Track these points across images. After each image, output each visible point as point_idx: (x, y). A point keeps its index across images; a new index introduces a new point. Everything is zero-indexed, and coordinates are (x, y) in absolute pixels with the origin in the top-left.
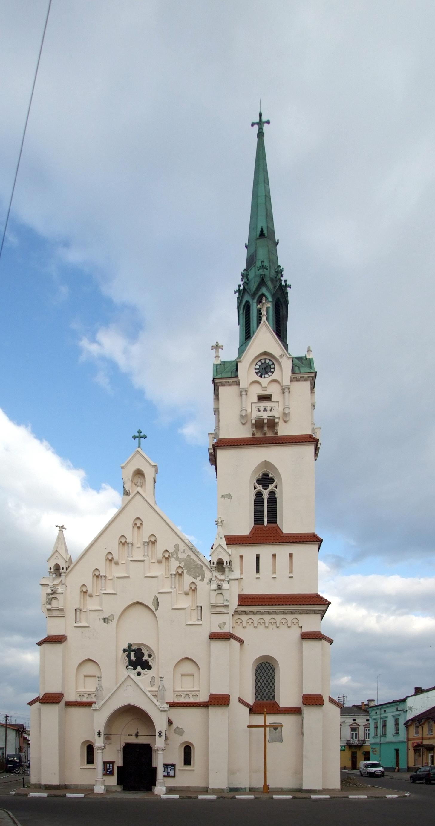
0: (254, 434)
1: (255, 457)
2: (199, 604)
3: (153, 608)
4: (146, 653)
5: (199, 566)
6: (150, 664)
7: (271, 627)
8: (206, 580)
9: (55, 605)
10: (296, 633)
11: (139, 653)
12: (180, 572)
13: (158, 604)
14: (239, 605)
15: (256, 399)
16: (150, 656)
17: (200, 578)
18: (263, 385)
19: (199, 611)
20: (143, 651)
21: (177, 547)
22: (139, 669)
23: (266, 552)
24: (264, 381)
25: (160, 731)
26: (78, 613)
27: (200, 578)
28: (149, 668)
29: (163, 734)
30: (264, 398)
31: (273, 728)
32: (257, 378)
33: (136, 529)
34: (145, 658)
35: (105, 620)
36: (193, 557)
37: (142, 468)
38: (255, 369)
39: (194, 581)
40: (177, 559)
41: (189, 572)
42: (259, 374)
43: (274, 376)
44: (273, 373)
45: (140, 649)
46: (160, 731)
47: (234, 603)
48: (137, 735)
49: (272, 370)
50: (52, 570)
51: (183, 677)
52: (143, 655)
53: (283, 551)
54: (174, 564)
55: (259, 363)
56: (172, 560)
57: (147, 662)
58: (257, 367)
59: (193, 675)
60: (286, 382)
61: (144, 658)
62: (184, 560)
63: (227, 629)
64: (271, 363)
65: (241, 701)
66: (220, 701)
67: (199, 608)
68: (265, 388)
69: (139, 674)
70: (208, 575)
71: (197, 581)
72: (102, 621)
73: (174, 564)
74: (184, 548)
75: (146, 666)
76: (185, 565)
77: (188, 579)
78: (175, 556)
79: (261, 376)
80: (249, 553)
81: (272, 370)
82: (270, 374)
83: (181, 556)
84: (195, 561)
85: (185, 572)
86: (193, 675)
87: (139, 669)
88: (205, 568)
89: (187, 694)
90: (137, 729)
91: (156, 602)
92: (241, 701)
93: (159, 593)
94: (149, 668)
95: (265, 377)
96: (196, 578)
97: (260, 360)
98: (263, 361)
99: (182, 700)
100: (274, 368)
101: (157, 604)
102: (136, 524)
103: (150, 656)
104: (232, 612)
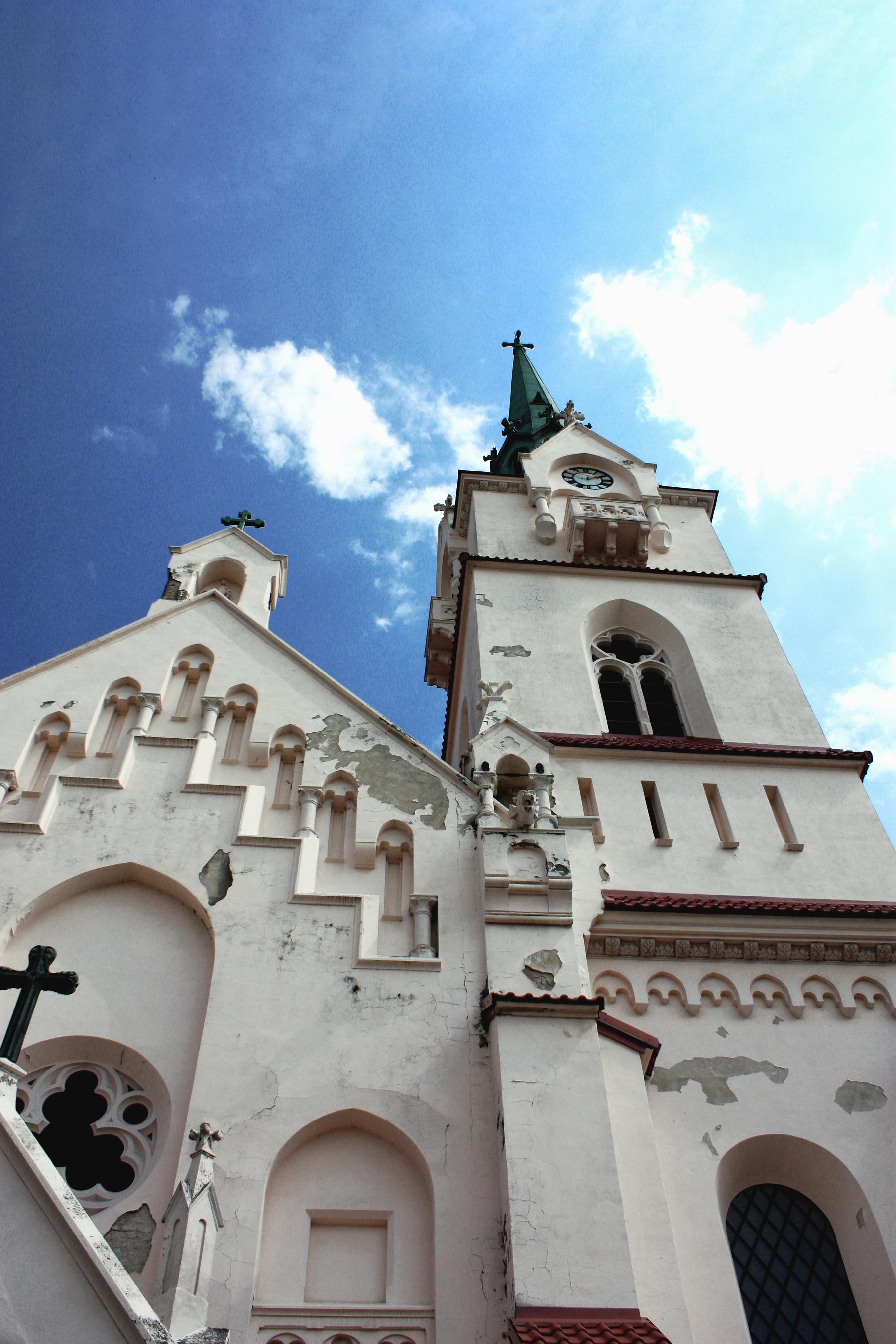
2: (421, 887)
3: (201, 894)
4: (117, 1103)
5: (423, 778)
6: (129, 1154)
7: (765, 1016)
13: (227, 879)
16: (136, 1113)
17: (428, 810)
19: (423, 921)
20: (102, 1087)
27: (428, 810)
33: (180, 681)
34: (111, 1120)
36: (397, 750)
39: (401, 817)
40: (334, 750)
47: (585, 906)
51: (326, 1235)
52: (100, 1106)
57: (112, 1144)
59: (378, 1223)
61: (101, 1124)
62: (358, 755)
67: (424, 908)
71: (415, 821)
74: (365, 727)
76: (357, 770)
85: (363, 791)
86: (378, 1223)
91: (215, 872)
101: (223, 878)
103: (136, 1113)
104: (582, 927)
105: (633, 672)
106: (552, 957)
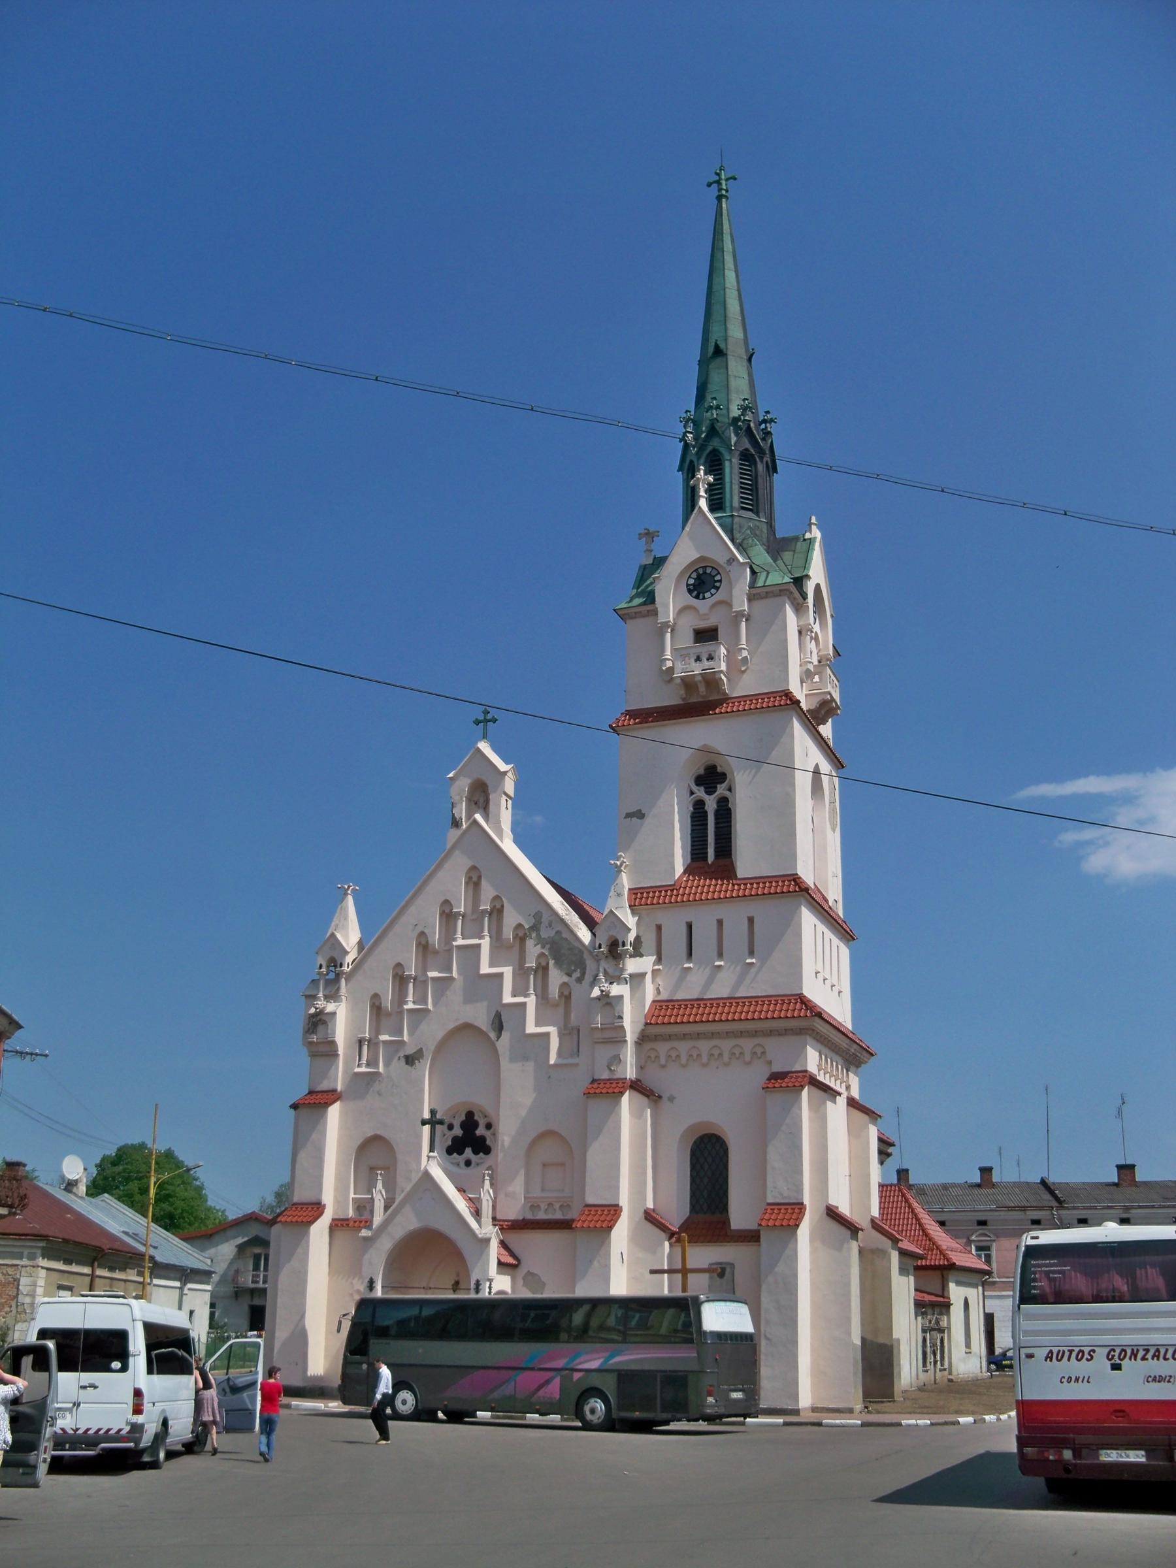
0: (684, 699)
4: (482, 1123)
6: (488, 1142)
8: (588, 978)
10: (760, 1074)
11: (470, 1123)
12: (544, 964)
14: (646, 1024)
15: (687, 640)
16: (489, 1126)
18: (701, 612)
19: (575, 1037)
20: (476, 1118)
22: (468, 1152)
24: (702, 605)
25: (478, 1281)
26: (365, 1048)
27: (577, 974)
28: (487, 1150)
30: (706, 635)
31: (715, 1275)
32: (691, 601)
35: (410, 1060)
37: (484, 778)
38: (688, 585)
40: (541, 941)
41: (559, 963)
42: (695, 593)
43: (720, 595)
44: (717, 588)
45: (470, 1115)
46: (478, 1281)
48: (456, 1287)
49: (717, 584)
50: (324, 969)
52: (476, 1125)
53: (735, 915)
55: (694, 575)
56: (530, 943)
57: (483, 1139)
58: (691, 581)
59: (562, 1165)
60: (741, 603)
64: (714, 573)
67: (575, 1032)
69: (468, 1163)
70: (590, 964)
72: (403, 1061)
75: (482, 1147)
77: (556, 977)
78: (534, 935)
79: (697, 597)
81: (717, 584)
82: (713, 591)
83: (546, 933)
84: (569, 943)
85: (551, 962)
87: (468, 1152)
88: (586, 955)
89: (550, 1204)
90: (458, 1275)
94: (487, 1150)
95: (704, 598)
96: (569, 975)
97: (696, 570)
98: (701, 571)
99: (541, 1216)
100: (720, 581)
102: (471, 878)
105: (711, 805)
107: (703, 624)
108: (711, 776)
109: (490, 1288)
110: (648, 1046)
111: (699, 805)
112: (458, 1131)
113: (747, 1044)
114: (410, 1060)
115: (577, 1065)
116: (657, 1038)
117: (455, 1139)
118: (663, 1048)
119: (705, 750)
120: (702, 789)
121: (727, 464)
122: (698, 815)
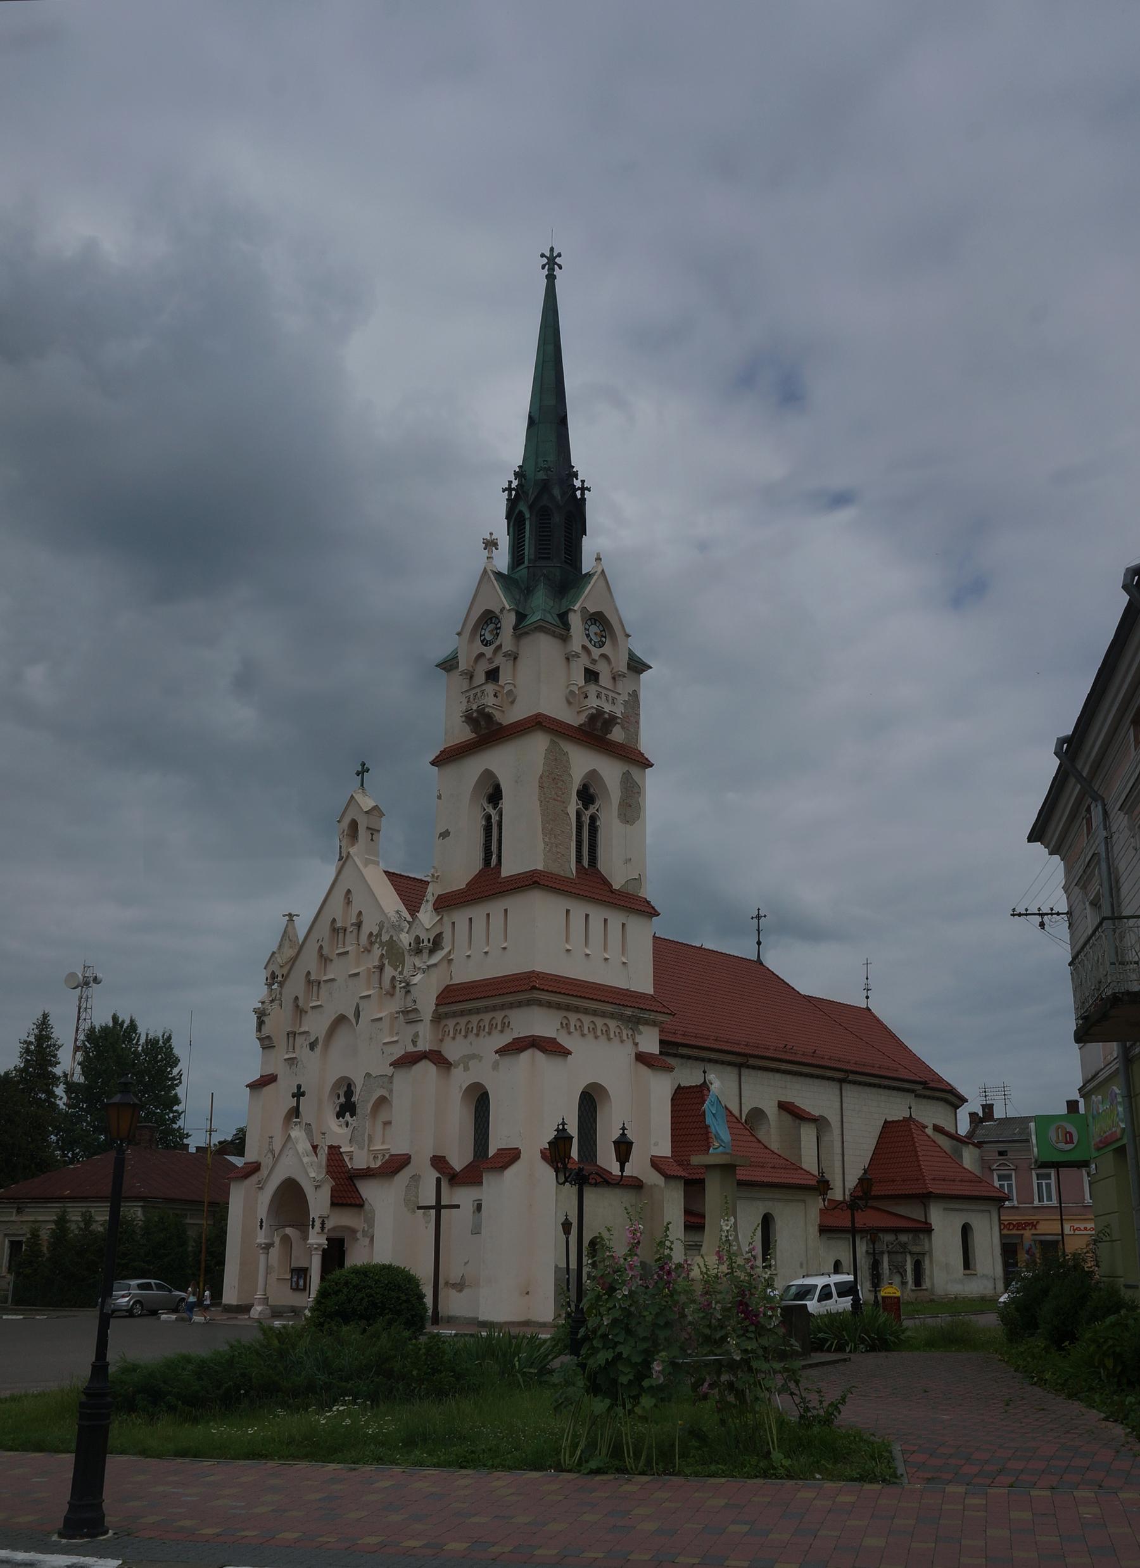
1: (473, 768)
9: (266, 1030)
11: (349, 1093)
14: (437, 1005)
21: (381, 926)
23: (478, 913)
24: (489, 651)
26: (291, 1039)
29: (318, 1224)
40: (382, 945)
45: (349, 1086)
54: (377, 951)
63: (423, 1045)
65: (439, 1162)
66: (395, 1165)
68: (491, 661)
73: (377, 951)
77: (389, 971)
80: (460, 917)
83: (385, 938)
88: (406, 953)
92: (439, 1162)
93: (361, 998)
101: (357, 1014)
106: (417, 1035)
107: (493, 666)
108: (495, 796)
109: (323, 1224)
110: (444, 1022)
111: (488, 818)
112: (342, 1100)
113: (499, 1016)
114: (312, 1046)
115: (397, 1042)
116: (447, 1016)
117: (341, 1106)
118: (451, 1023)
119: (488, 775)
120: (491, 806)
121: (527, 523)
122: (488, 829)
